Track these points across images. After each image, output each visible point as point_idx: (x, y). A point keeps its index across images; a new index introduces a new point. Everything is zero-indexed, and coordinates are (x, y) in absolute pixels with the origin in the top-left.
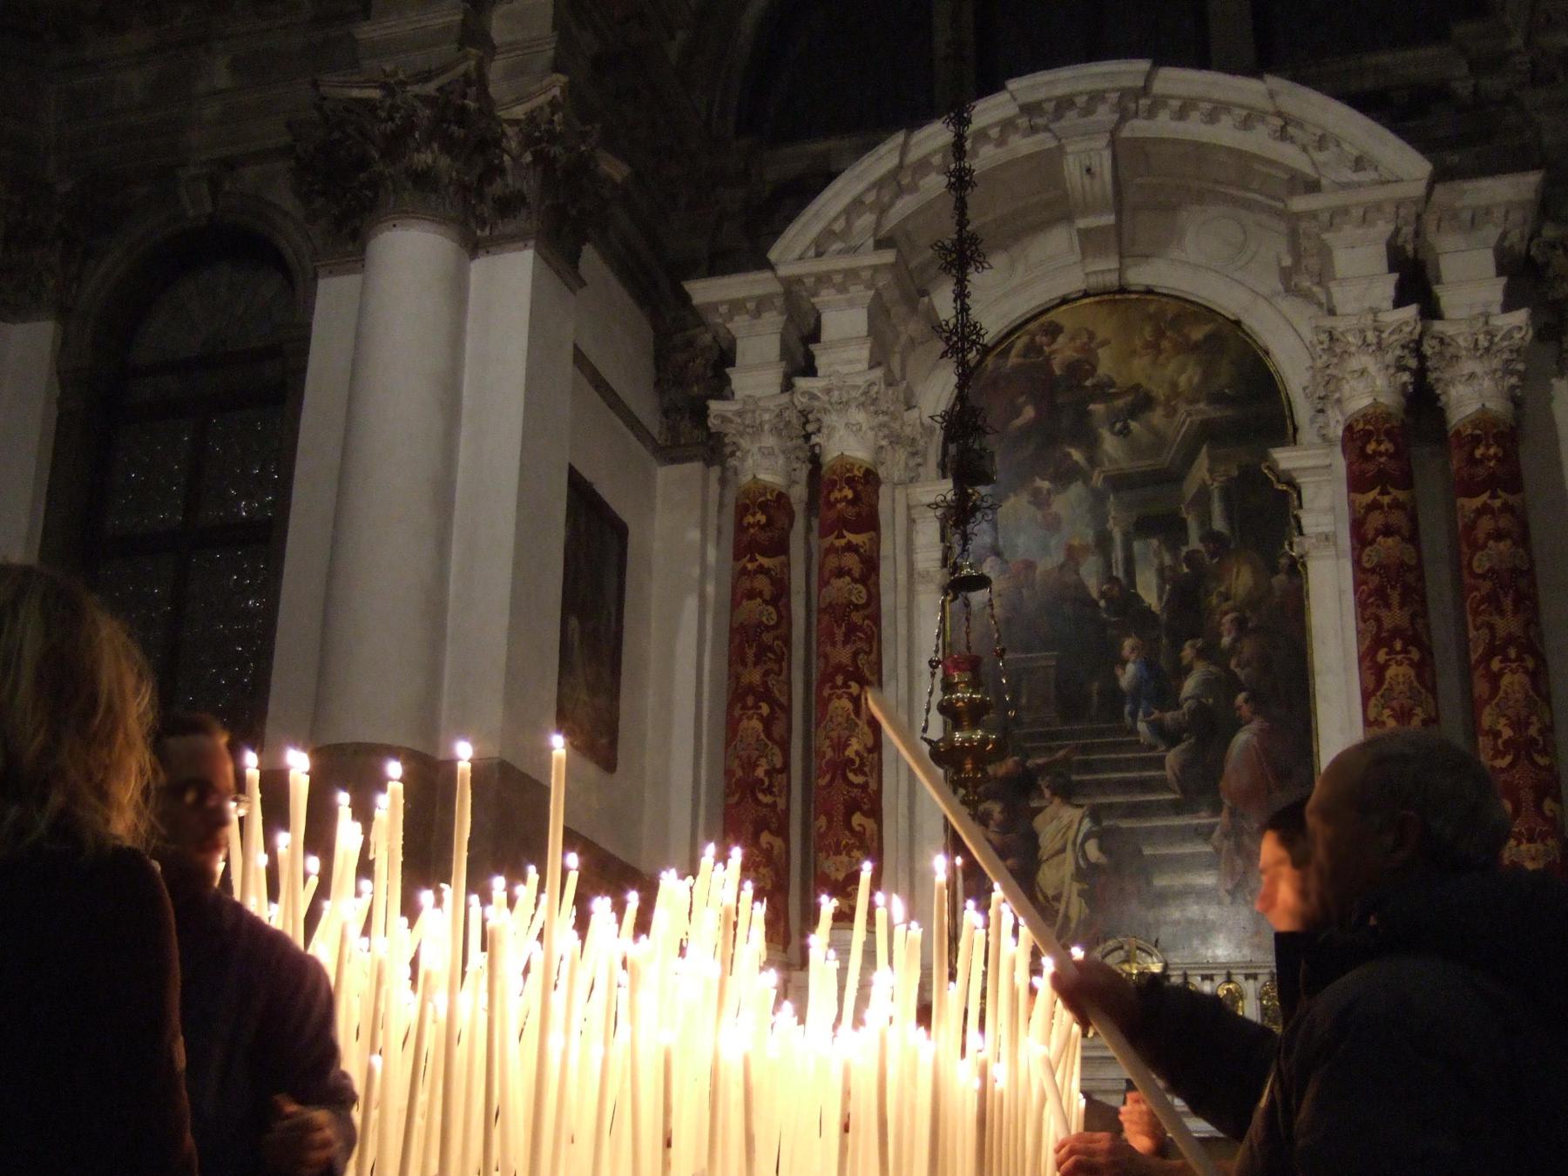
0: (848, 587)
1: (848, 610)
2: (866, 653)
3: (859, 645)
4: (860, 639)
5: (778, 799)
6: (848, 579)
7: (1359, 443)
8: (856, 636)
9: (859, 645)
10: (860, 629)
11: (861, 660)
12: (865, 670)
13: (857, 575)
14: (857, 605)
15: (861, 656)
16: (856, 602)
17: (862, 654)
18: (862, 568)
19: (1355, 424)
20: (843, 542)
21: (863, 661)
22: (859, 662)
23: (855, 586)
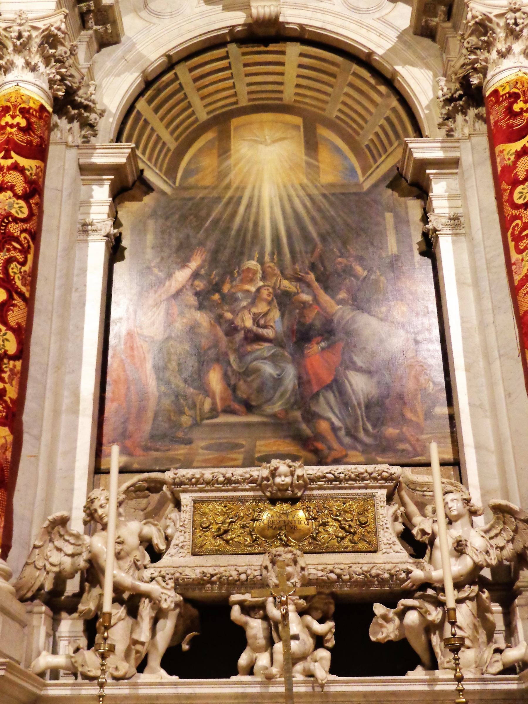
0: (9, 200)
1: (6, 220)
2: (19, 263)
3: (13, 253)
4: (15, 248)
5: (8, 386)
6: (9, 193)
7: (505, 104)
8: (11, 245)
9: (13, 253)
10: (17, 239)
11: (12, 269)
12: (17, 280)
13: (19, 192)
14: (16, 217)
15: (13, 265)
16: (16, 215)
17: (14, 263)
18: (25, 188)
19: (500, 90)
20: (9, 162)
21: (15, 270)
22: (10, 271)
23: (16, 201)
